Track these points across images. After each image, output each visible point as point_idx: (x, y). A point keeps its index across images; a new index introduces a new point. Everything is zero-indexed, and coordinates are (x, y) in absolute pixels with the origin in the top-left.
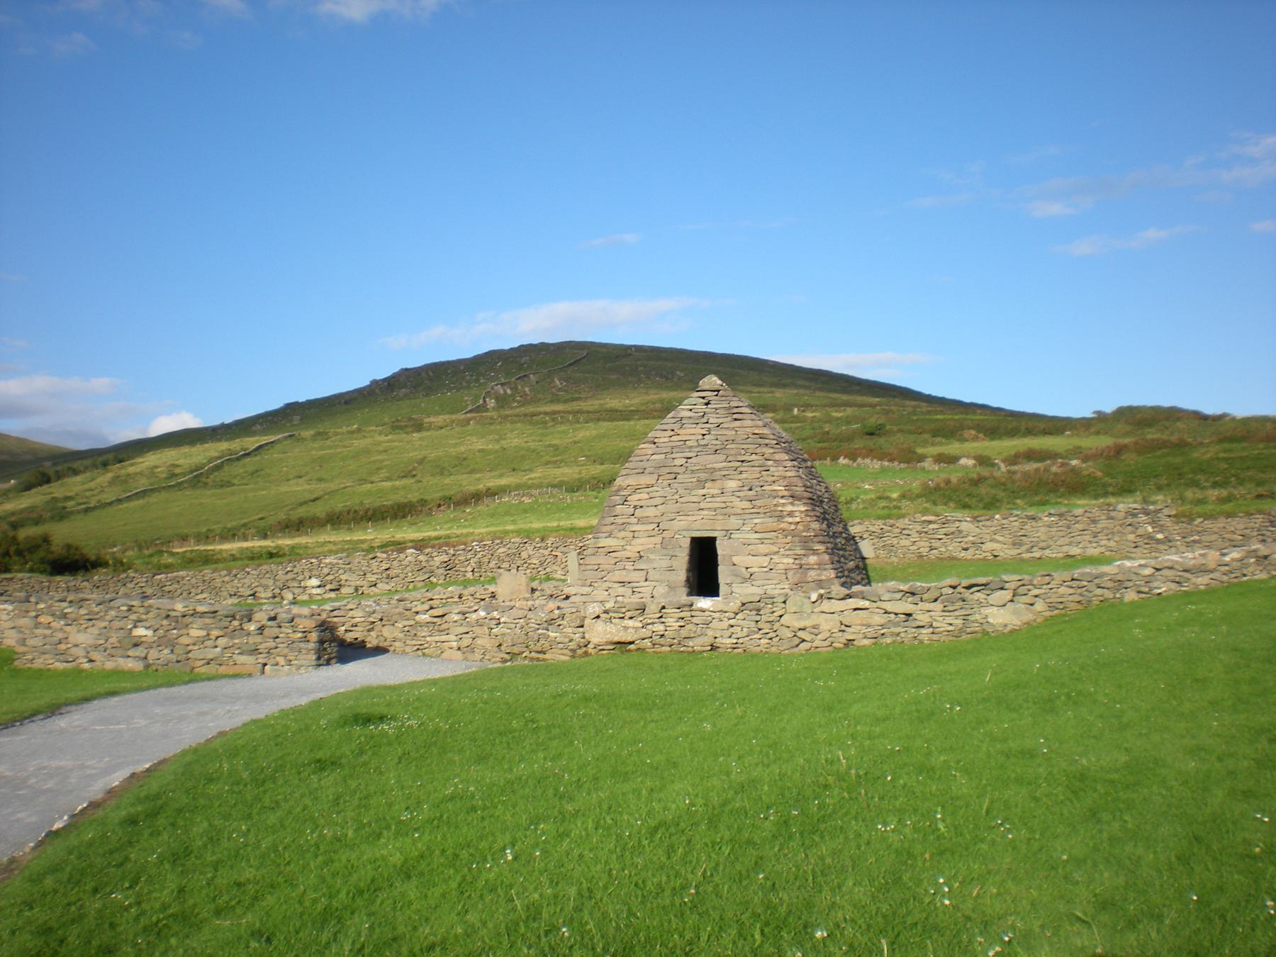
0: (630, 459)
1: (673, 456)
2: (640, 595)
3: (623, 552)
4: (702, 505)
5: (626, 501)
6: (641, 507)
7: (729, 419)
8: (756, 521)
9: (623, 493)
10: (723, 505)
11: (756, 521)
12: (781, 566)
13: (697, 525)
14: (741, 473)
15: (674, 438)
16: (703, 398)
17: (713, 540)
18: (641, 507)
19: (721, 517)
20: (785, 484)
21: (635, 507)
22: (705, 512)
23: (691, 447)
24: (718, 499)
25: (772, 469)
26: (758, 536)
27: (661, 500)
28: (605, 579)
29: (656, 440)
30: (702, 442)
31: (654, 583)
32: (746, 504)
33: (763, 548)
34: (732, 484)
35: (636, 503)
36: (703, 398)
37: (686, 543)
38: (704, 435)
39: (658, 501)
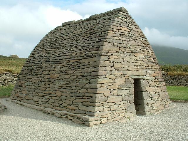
0: (107, 37)
1: (123, 39)
2: (121, 109)
3: (113, 86)
4: (136, 64)
5: (109, 59)
6: (115, 62)
7: (134, 27)
8: (150, 72)
9: (107, 55)
10: (140, 64)
11: (150, 72)
12: (158, 91)
13: (136, 73)
14: (142, 51)
15: (120, 30)
16: (124, 15)
17: (140, 79)
18: (115, 62)
19: (140, 70)
20: (153, 58)
21: (113, 62)
22: (136, 67)
23: (127, 36)
24: (139, 62)
25: (150, 51)
26: (150, 78)
27: (122, 60)
28: (107, 101)
29: (114, 30)
30: (130, 35)
31: (126, 102)
32: (146, 65)
33: (153, 84)
34: (142, 55)
35: (113, 60)
36: (124, 15)
37: (133, 81)
38: (129, 32)
39: (122, 60)
